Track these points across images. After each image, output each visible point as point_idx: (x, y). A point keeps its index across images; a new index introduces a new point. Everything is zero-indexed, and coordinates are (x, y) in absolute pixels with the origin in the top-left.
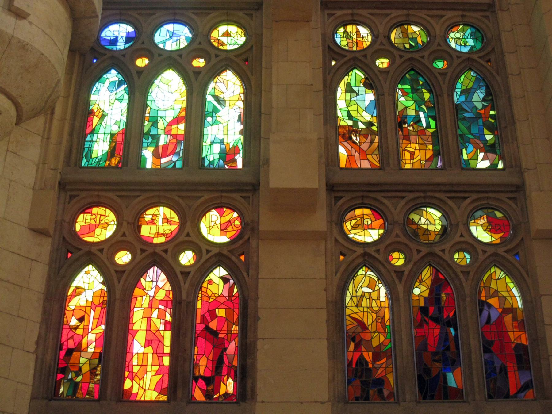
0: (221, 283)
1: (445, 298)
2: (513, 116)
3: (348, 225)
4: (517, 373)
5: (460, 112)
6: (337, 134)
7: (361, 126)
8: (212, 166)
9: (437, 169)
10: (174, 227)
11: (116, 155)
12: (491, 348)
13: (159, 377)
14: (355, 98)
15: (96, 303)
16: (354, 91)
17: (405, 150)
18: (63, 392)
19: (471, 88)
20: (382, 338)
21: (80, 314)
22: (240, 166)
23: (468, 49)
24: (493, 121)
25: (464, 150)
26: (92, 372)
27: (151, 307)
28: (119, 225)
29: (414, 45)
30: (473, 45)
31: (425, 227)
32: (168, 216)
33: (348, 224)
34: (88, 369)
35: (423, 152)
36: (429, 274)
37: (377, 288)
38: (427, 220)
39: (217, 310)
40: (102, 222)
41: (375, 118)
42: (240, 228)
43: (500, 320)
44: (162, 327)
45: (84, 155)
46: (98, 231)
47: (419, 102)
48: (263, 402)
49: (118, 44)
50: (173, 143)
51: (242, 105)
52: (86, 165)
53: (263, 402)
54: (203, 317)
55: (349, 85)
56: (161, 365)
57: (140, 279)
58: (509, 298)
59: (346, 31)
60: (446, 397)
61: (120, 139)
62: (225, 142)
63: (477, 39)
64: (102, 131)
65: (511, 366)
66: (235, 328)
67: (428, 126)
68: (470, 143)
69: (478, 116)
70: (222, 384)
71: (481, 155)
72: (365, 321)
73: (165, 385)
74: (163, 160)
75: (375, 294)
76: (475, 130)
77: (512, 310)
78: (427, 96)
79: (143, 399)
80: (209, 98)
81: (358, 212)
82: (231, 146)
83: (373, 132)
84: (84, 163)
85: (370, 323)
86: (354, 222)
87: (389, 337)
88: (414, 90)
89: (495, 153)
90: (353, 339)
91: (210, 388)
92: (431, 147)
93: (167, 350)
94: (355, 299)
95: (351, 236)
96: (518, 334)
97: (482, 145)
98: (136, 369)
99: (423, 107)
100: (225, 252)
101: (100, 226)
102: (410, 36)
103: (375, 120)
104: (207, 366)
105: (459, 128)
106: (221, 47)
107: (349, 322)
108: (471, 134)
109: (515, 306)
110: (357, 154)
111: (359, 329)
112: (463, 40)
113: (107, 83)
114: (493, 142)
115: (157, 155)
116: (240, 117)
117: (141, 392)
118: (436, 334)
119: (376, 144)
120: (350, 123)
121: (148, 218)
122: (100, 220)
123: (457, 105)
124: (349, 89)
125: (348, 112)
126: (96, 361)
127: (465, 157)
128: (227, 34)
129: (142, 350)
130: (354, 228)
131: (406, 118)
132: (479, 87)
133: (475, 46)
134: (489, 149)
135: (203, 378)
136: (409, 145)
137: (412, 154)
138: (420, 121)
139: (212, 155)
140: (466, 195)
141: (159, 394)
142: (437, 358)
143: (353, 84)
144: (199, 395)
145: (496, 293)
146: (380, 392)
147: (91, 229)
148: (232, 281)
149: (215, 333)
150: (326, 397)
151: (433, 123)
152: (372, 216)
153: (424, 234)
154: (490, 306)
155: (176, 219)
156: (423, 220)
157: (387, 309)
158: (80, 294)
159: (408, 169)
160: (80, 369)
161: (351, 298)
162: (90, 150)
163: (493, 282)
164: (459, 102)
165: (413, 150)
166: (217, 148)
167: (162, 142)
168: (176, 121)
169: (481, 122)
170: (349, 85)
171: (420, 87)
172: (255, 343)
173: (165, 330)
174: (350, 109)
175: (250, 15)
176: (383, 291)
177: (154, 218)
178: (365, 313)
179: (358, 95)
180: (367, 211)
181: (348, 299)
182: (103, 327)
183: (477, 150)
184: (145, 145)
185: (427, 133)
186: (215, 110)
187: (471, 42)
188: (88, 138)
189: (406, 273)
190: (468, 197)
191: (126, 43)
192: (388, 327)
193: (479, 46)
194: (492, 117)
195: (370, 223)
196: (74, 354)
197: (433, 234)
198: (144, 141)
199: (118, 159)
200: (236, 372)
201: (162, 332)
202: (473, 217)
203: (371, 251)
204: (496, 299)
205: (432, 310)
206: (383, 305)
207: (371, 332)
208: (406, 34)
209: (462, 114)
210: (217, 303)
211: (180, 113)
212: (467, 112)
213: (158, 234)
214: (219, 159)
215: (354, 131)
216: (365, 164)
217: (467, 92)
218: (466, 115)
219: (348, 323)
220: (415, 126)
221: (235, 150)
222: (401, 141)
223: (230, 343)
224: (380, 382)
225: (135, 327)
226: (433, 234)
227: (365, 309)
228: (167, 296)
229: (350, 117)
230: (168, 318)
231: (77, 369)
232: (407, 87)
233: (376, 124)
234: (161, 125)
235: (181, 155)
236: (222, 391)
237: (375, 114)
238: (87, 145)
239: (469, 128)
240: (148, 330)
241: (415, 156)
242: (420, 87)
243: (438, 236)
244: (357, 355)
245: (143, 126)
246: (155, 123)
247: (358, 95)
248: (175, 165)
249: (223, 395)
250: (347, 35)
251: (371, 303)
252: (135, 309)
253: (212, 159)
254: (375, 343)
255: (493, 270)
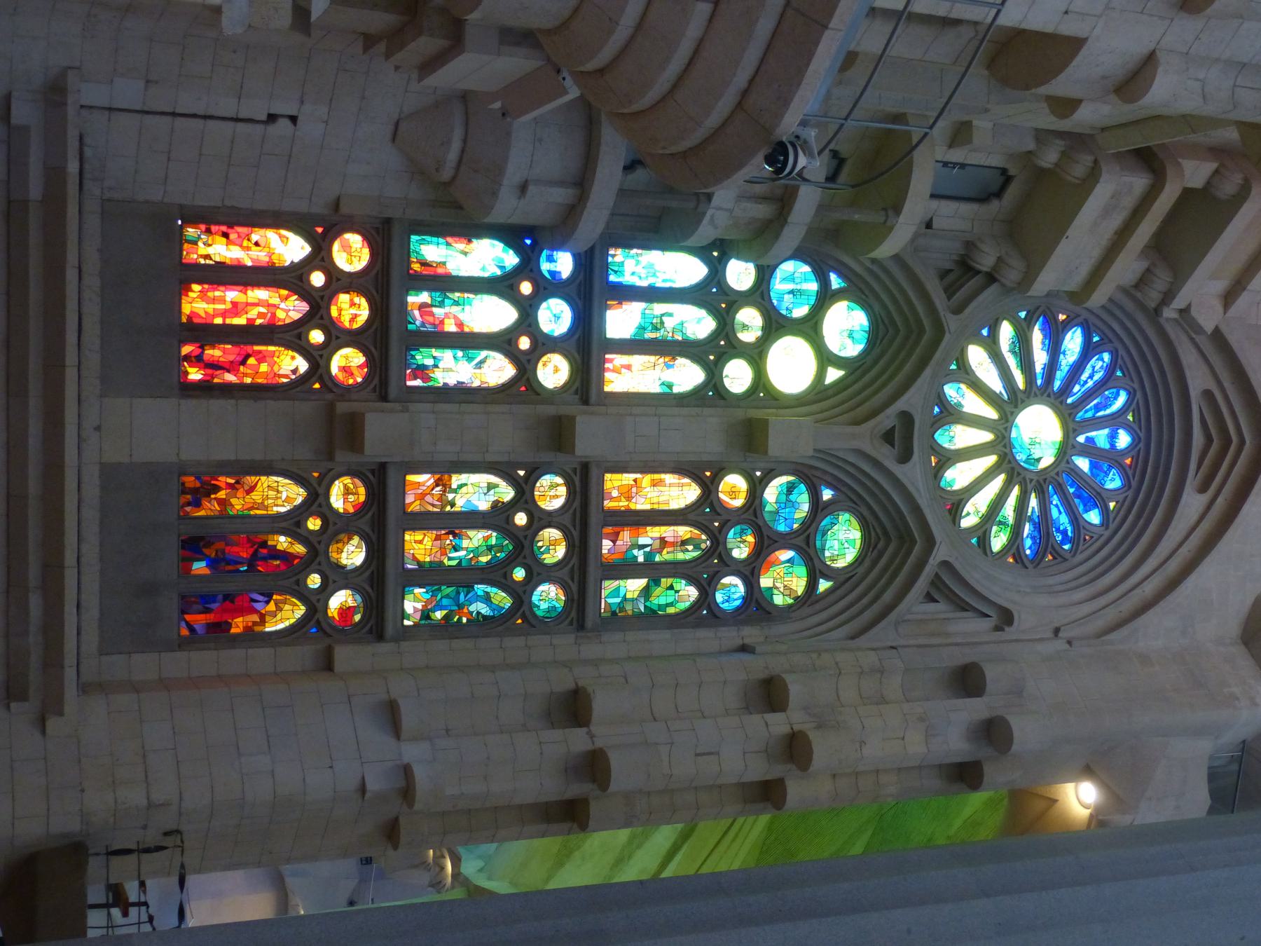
0: (293, 368)
1: (275, 563)
2: (457, 638)
3: (347, 480)
4: (205, 622)
5: (465, 589)
6: (442, 473)
7: (450, 496)
8: (409, 358)
9: (403, 564)
10: (347, 324)
11: (423, 268)
12: (227, 602)
13: (203, 315)
14: (481, 491)
15: (273, 257)
16: (489, 490)
17: (425, 535)
18: (188, 231)
19: (492, 602)
20: (238, 507)
21: (262, 243)
22: (410, 383)
23: (537, 603)
24: (455, 620)
25: (424, 590)
26: (207, 257)
27: (269, 305)
28: (350, 274)
29: (541, 550)
30: (541, 608)
31: (345, 550)
32: (358, 319)
33: (349, 481)
34: (210, 253)
35: (423, 552)
36: (298, 550)
37: (286, 504)
38: (353, 552)
39: (266, 364)
40: (353, 257)
41: (459, 509)
42: (346, 384)
43: (255, 611)
44: (249, 316)
45: (424, 237)
46: (344, 255)
47: (476, 552)
48: (179, 405)
49: (548, 264)
50: (434, 321)
51: (476, 384)
52: (411, 240)
53: (179, 405)
54: (260, 352)
55: (496, 486)
56: (214, 316)
57: (296, 294)
58: (274, 620)
59: (558, 485)
60: (183, 559)
61: (440, 271)
62: (435, 369)
63: (548, 612)
64: (450, 252)
65: (210, 618)
66: (248, 380)
67: (450, 559)
68: (432, 596)
69: (461, 607)
70: (198, 369)
71: (419, 606)
72: (254, 493)
73: (196, 320)
74: (417, 313)
75: (280, 502)
76: (445, 602)
77: (263, 621)
78: (484, 559)
79: (183, 301)
80: (484, 353)
81: (362, 490)
82: (432, 375)
83: (443, 507)
84: (414, 238)
85: (253, 497)
86: (351, 486)
87: (240, 513)
88: (490, 548)
89: (421, 619)
90: (238, 482)
91: (193, 359)
92: (428, 559)
93: (228, 321)
94: (276, 484)
95: (337, 482)
96: (241, 626)
97: (429, 607)
98: (210, 294)
99: (472, 555)
100: (320, 371)
101: (350, 257)
102: (551, 547)
103: (456, 509)
104: (213, 356)
105: (448, 587)
106: (540, 365)
107: (254, 479)
108: (442, 598)
109: (267, 624)
110: (420, 491)
111: (247, 487)
112: (547, 599)
113: (504, 256)
114: (432, 618)
115: (422, 306)
116: (463, 383)
117: (190, 300)
118: (241, 554)
119: (431, 509)
120: (454, 486)
121: (357, 300)
122: (355, 256)
123: (473, 587)
124: (491, 487)
125: (466, 485)
126: (218, 259)
127: (417, 591)
128: (556, 370)
129: (228, 299)
130: (345, 486)
131: (459, 539)
132: (493, 610)
133: (539, 609)
134: (426, 615)
135: (202, 353)
136: (429, 539)
137: (421, 542)
138: (456, 550)
139: (421, 357)
140: (375, 589)
141: (188, 316)
142: (219, 553)
143: (497, 490)
144: (186, 349)
145: (279, 609)
146: (189, 504)
147: (346, 248)
148: (293, 377)
149: (243, 362)
150: (184, 457)
151: (454, 563)
152: (357, 502)
153: (338, 548)
154: (268, 602)
155: (355, 326)
156: (352, 548)
157: (265, 512)
158: (283, 242)
159: (404, 536)
160: (210, 245)
161: (276, 482)
162: (429, 243)
163: (290, 607)
164: (476, 589)
165: (424, 542)
166: (429, 362)
167: (435, 310)
168: (460, 324)
169: (456, 608)
170: (496, 486)
171: (493, 553)
172: (232, 398)
173: (248, 319)
174: (470, 486)
175: (576, 393)
176: (283, 510)
177: (357, 306)
178: (262, 494)
179: (485, 494)
180: (362, 498)
181: (275, 478)
182: (249, 263)
183: (425, 602)
184: (433, 294)
185: (443, 557)
186: (470, 359)
187: (544, 606)
188: (441, 240)
189: (299, 530)
190: (373, 589)
191: (549, 272)
192: (249, 513)
193: (540, 613)
194: (460, 619)
195: (350, 500)
196: (224, 240)
197: (338, 556)
198: (438, 294)
199: (419, 270)
200: (208, 381)
201: (245, 316)
202: (354, 593)
203: (321, 499)
204: (274, 609)
205: (264, 551)
206: (269, 509)
207: (244, 498)
208: (554, 543)
209: (463, 591)
210: (272, 365)
211: (468, 326)
212: (465, 597)
213: (340, 310)
214: (418, 364)
215: (446, 489)
216: (409, 499)
217: (487, 599)
218: (462, 596)
219: (253, 478)
220: (450, 547)
221: (426, 379)
222: (435, 532)
223: (235, 376)
224: (197, 504)
225: (249, 292)
226: (338, 556)
227: (266, 494)
228: (279, 320)
229: (461, 486)
230: (258, 322)
231: (210, 242)
232: (493, 541)
233: (453, 510)
234: (455, 310)
235: (422, 329)
236: (190, 370)
237: (463, 509)
238: (435, 239)
239: (447, 596)
240: (248, 304)
241: (419, 545)
242: (493, 553)
243: (336, 562)
244: (223, 485)
245: (453, 291)
246: (456, 303)
247: (485, 494)
248: (411, 323)
249: (187, 371)
250: (553, 486)
251: (272, 499)
252: (267, 292)
253: (417, 357)
254: (233, 501)
255: (303, 608)
